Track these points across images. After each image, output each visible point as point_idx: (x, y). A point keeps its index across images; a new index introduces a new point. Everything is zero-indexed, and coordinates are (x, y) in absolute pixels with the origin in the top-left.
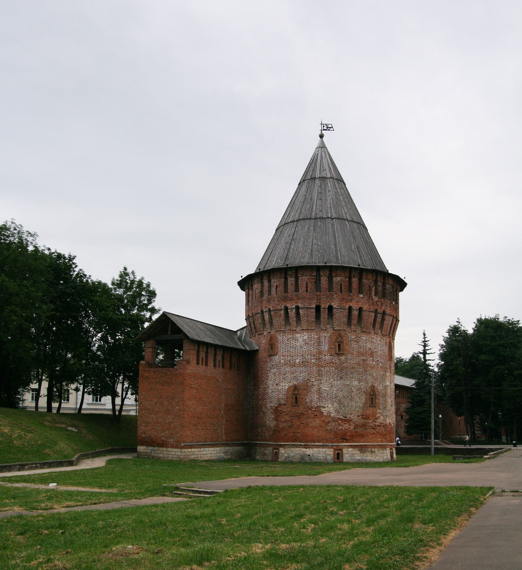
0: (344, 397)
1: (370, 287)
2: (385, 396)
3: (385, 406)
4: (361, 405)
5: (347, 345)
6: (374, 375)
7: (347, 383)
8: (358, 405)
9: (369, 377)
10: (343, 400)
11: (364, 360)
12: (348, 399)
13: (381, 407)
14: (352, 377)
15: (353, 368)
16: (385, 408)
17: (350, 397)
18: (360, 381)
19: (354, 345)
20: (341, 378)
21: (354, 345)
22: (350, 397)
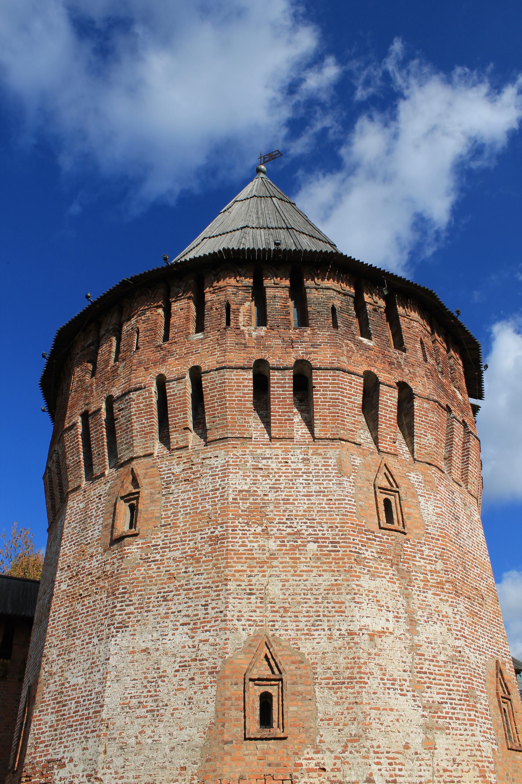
0: (126, 706)
1: (228, 307)
2: (349, 680)
3: (353, 729)
4: (198, 740)
5: (153, 501)
6: (275, 590)
7: (143, 640)
8: (184, 735)
9: (237, 606)
10: (119, 721)
11: (215, 540)
12: (142, 712)
13: (328, 736)
14: (166, 616)
15: (172, 577)
16: (355, 739)
17: (151, 705)
18: (194, 625)
19: (181, 493)
20: (123, 626)
21: (181, 493)
22: (151, 705)
